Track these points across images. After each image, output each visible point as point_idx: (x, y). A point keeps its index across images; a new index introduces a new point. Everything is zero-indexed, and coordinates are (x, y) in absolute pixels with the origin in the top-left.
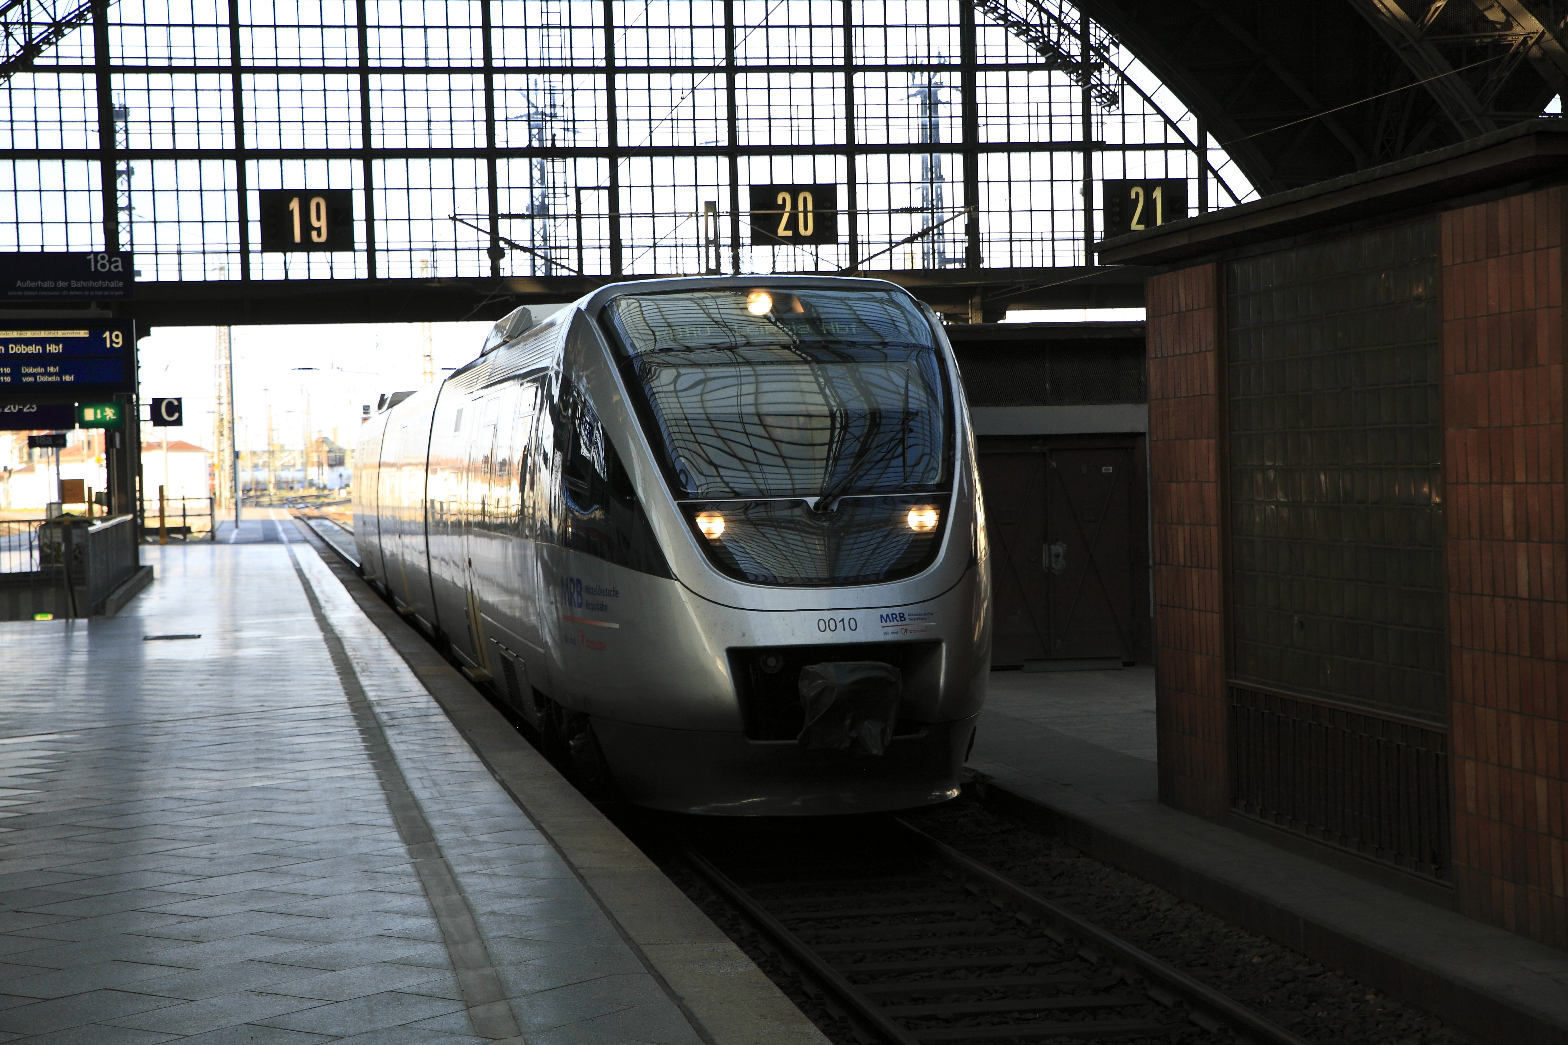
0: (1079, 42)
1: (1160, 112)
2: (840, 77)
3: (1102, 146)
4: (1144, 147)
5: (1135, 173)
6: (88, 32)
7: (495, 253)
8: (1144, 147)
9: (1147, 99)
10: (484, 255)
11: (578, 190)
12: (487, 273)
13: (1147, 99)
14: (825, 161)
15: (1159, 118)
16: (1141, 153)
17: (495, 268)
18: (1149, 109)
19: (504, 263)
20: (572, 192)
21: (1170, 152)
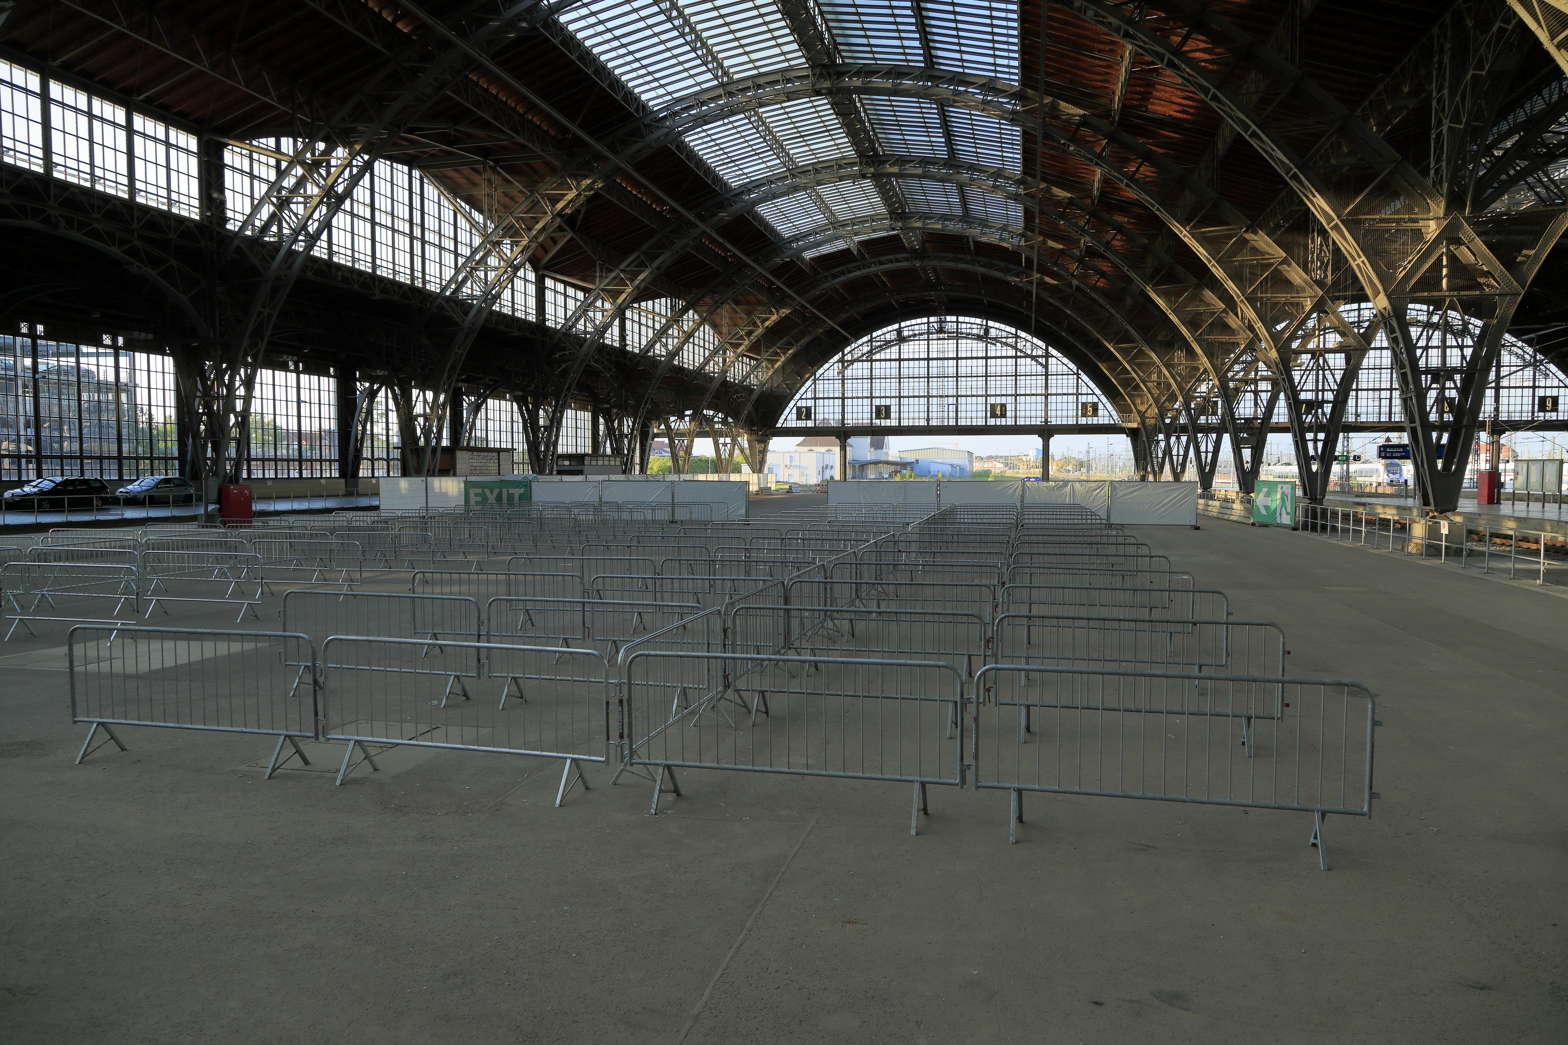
2: (1014, 378)
3: (1082, 394)
7: (928, 420)
17: (928, 423)
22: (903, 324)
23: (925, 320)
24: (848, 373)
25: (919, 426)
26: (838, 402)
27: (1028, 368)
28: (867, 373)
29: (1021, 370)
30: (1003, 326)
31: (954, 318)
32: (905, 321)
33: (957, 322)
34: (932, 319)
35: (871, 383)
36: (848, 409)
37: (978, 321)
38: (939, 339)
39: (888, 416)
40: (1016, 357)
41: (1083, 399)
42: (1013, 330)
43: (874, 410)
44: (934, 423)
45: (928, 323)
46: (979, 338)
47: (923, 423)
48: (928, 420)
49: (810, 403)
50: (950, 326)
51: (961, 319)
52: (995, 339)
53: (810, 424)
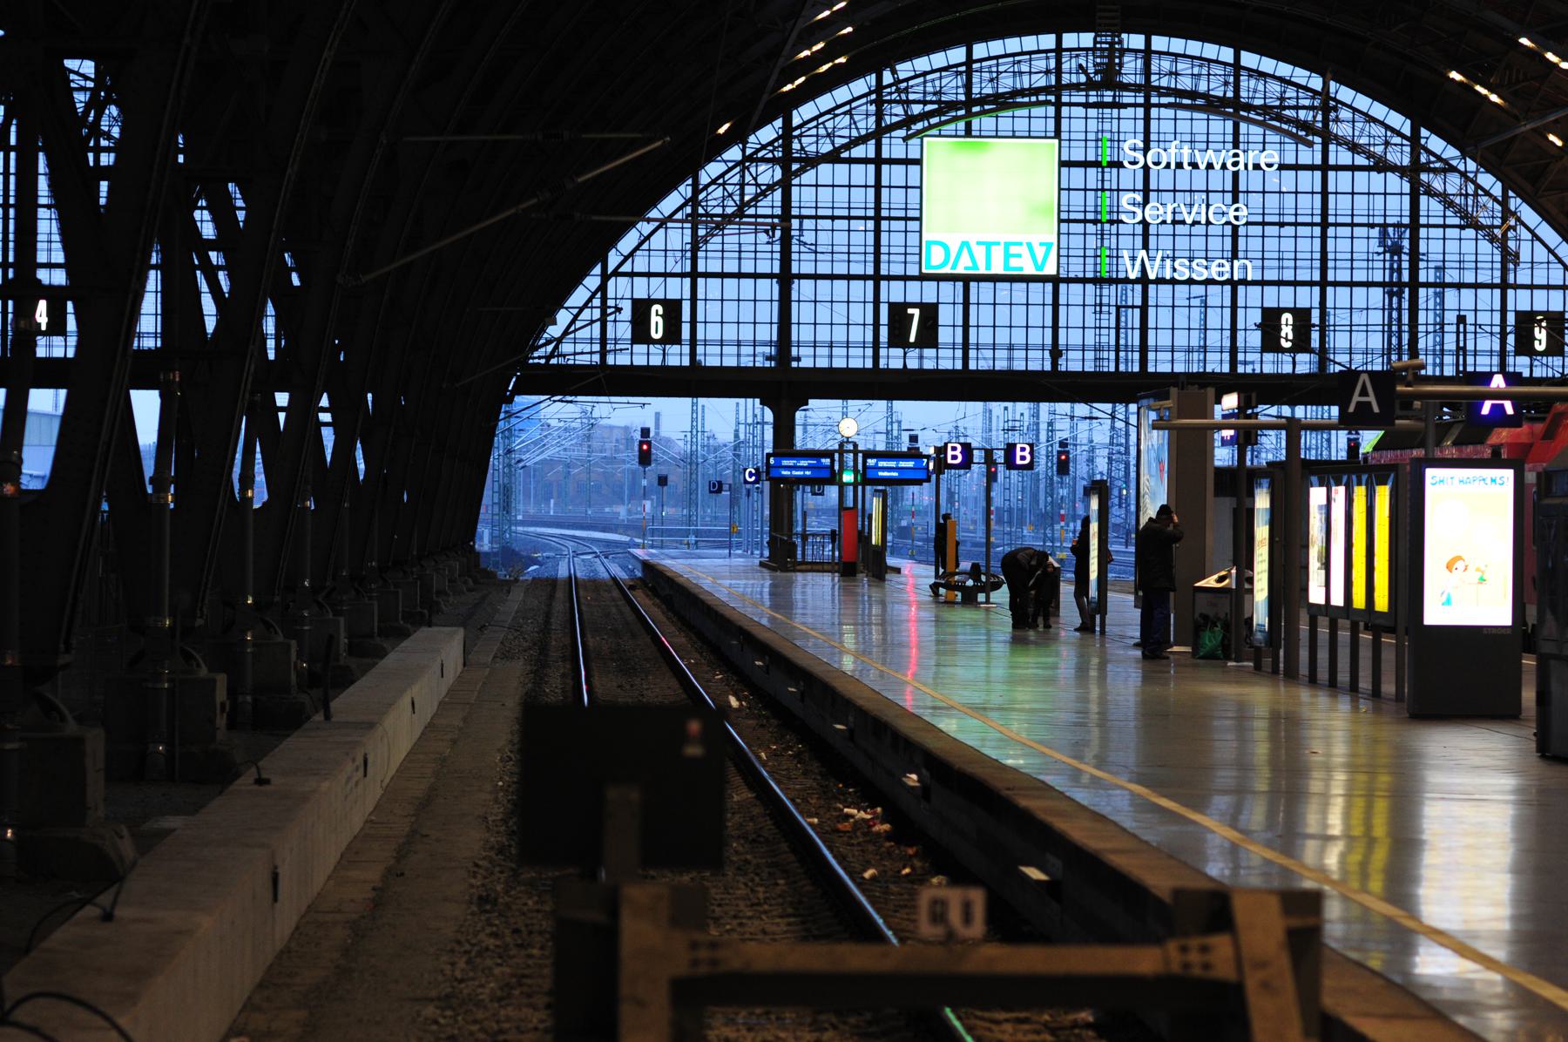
0: (1499, 208)
1: (1560, 261)
4: (1548, 287)
5: (1540, 305)
6: (778, 194)
7: (1056, 353)
8: (1548, 287)
9: (1551, 251)
10: (1047, 354)
11: (1118, 308)
12: (1048, 367)
13: (1551, 251)
14: (1303, 292)
15: (1560, 266)
16: (1545, 291)
17: (1055, 363)
18: (1552, 258)
19: (1062, 361)
20: (1113, 310)
21: (1535, 291)
22: (980, 50)
23: (1048, 41)
24: (802, 197)
25: (1027, 373)
26: (768, 289)
27: (1361, 202)
28: (862, 199)
29: (1340, 206)
30: (1284, 69)
31: (1136, 41)
32: (985, 38)
33: (1147, 53)
34: (1069, 40)
35: (877, 232)
36: (801, 312)
37: (1210, 50)
38: (1087, 105)
39: (929, 337)
40: (1325, 167)
41: (1521, 301)
42: (1316, 83)
43: (884, 319)
44: (1072, 363)
45: (1059, 50)
46: (1213, 105)
47: (1038, 362)
48: (1056, 353)
49: (677, 289)
50: (1131, 68)
51: (1159, 43)
52: (1265, 109)
53: (677, 356)
